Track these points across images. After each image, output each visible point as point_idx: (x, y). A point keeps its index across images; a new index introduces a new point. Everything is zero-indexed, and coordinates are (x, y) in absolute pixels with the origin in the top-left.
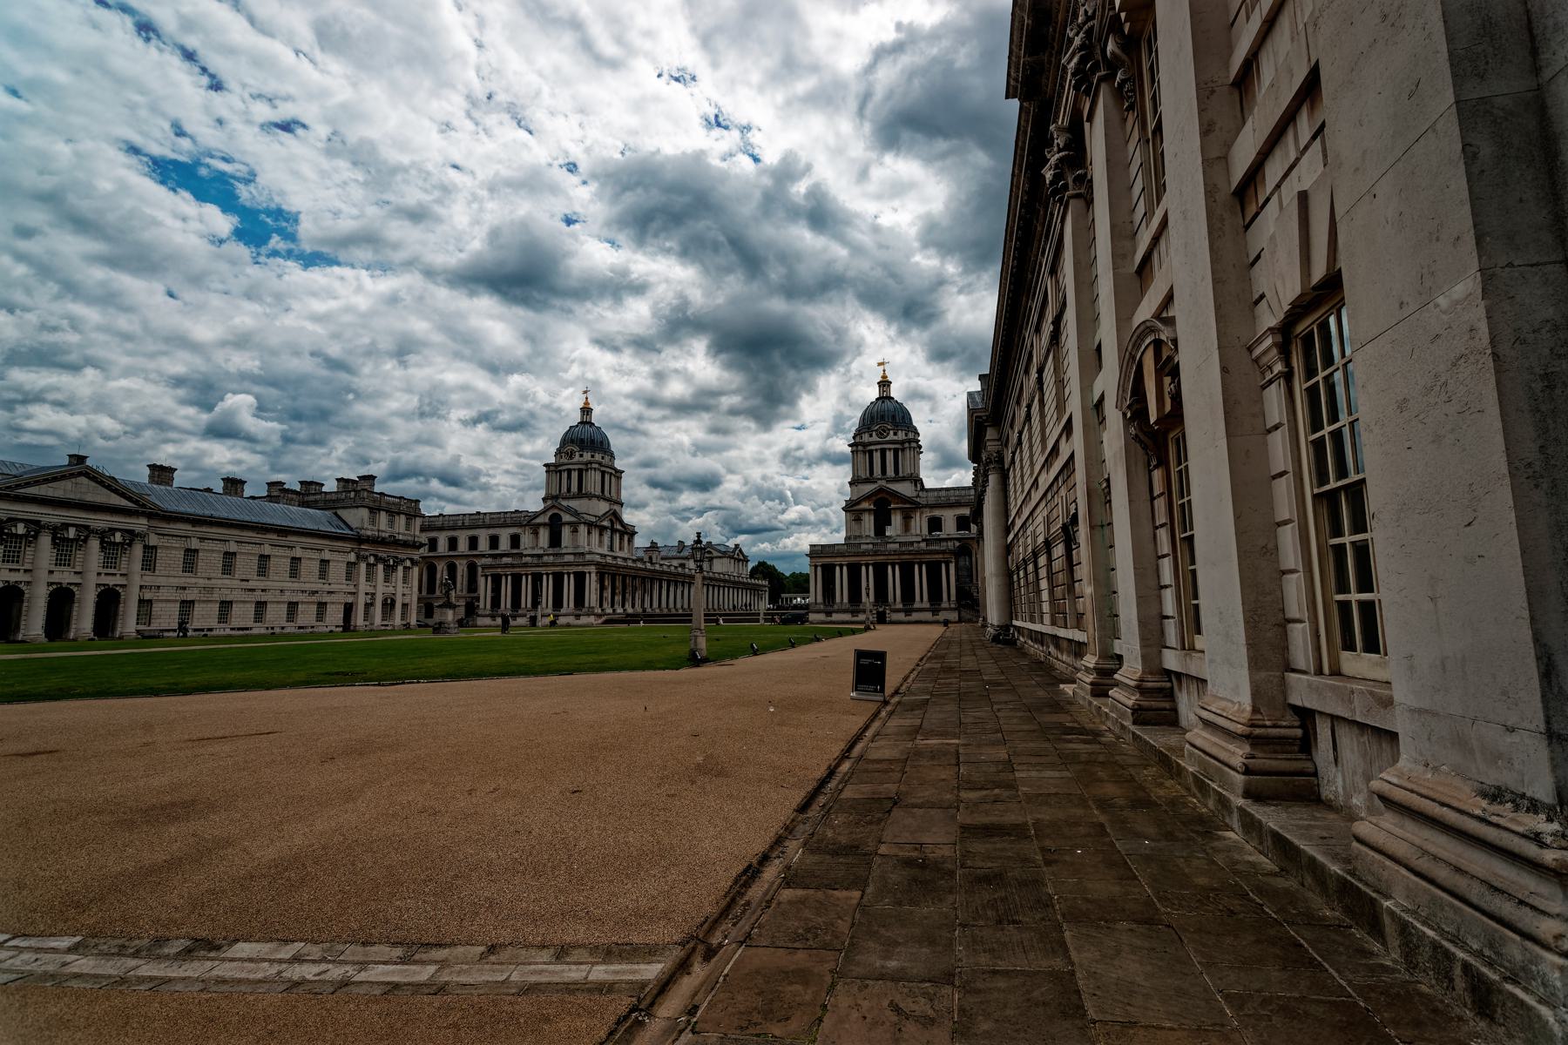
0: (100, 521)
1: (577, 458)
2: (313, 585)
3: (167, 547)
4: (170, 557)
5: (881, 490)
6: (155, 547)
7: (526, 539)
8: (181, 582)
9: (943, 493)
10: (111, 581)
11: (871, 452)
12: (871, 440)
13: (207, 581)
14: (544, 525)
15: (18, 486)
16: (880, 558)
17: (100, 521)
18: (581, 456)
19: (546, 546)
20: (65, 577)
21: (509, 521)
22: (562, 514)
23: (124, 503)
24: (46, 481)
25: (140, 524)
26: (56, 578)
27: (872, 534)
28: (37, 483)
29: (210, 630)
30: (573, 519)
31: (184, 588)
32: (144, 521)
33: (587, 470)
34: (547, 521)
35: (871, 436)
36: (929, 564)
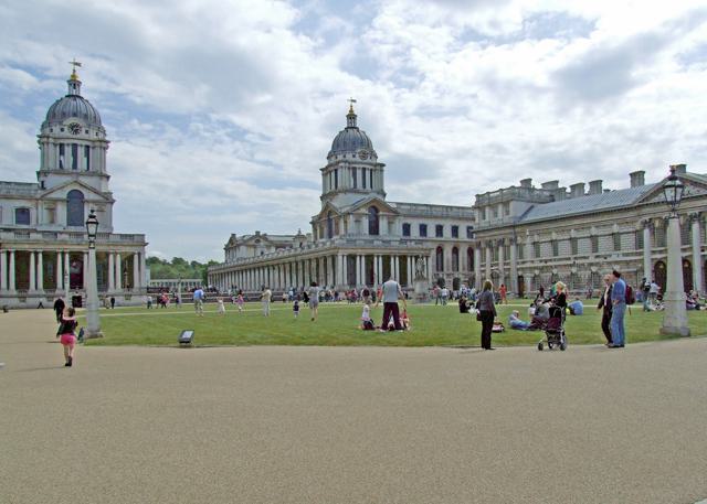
1: (82, 134)
5: (375, 200)
7: (39, 215)
9: (455, 210)
11: (354, 169)
12: (354, 159)
14: (62, 200)
16: (387, 252)
18: (87, 132)
19: (65, 225)
21: (13, 193)
22: (84, 191)
27: (367, 232)
30: (97, 197)
33: (93, 148)
34: (64, 196)
35: (354, 156)
36: (400, 257)
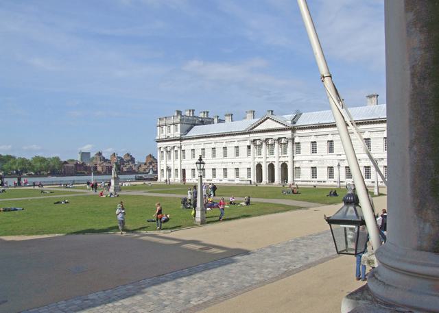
0: (276, 135)
2: (380, 155)
3: (304, 142)
4: (306, 147)
6: (299, 143)
8: (310, 158)
10: (283, 160)
13: (321, 157)
15: (253, 128)
17: (276, 135)
20: (271, 159)
23: (281, 126)
24: (259, 124)
25: (288, 134)
26: (268, 160)
28: (257, 125)
29: (324, 182)
31: (311, 161)
32: (290, 132)
